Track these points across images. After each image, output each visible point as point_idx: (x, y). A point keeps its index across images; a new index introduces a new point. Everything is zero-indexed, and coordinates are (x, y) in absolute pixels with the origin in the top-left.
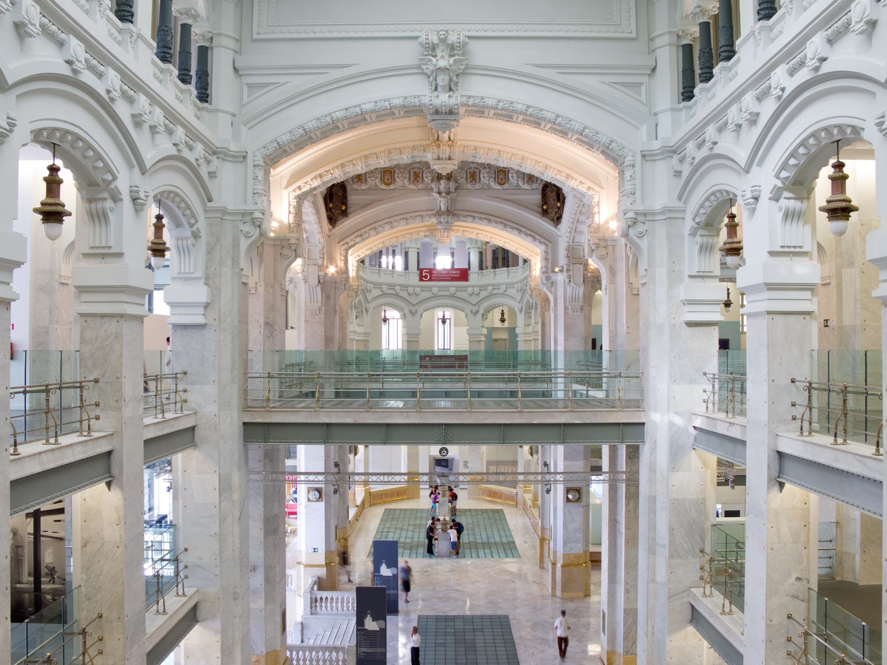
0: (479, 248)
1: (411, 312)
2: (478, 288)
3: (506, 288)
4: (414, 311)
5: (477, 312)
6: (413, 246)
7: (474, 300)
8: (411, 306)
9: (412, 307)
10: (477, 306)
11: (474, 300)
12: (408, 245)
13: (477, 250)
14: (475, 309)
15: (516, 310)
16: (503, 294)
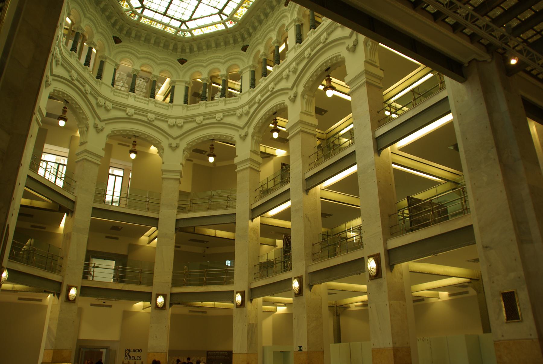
0: (186, 82)
1: (96, 127)
2: (182, 121)
3: (224, 116)
4: (100, 127)
5: (177, 147)
6: (111, 58)
7: (176, 132)
8: (97, 120)
9: (97, 121)
10: (178, 140)
11: (176, 132)
12: (106, 54)
13: (184, 84)
14: (174, 143)
15: (236, 138)
16: (219, 124)
